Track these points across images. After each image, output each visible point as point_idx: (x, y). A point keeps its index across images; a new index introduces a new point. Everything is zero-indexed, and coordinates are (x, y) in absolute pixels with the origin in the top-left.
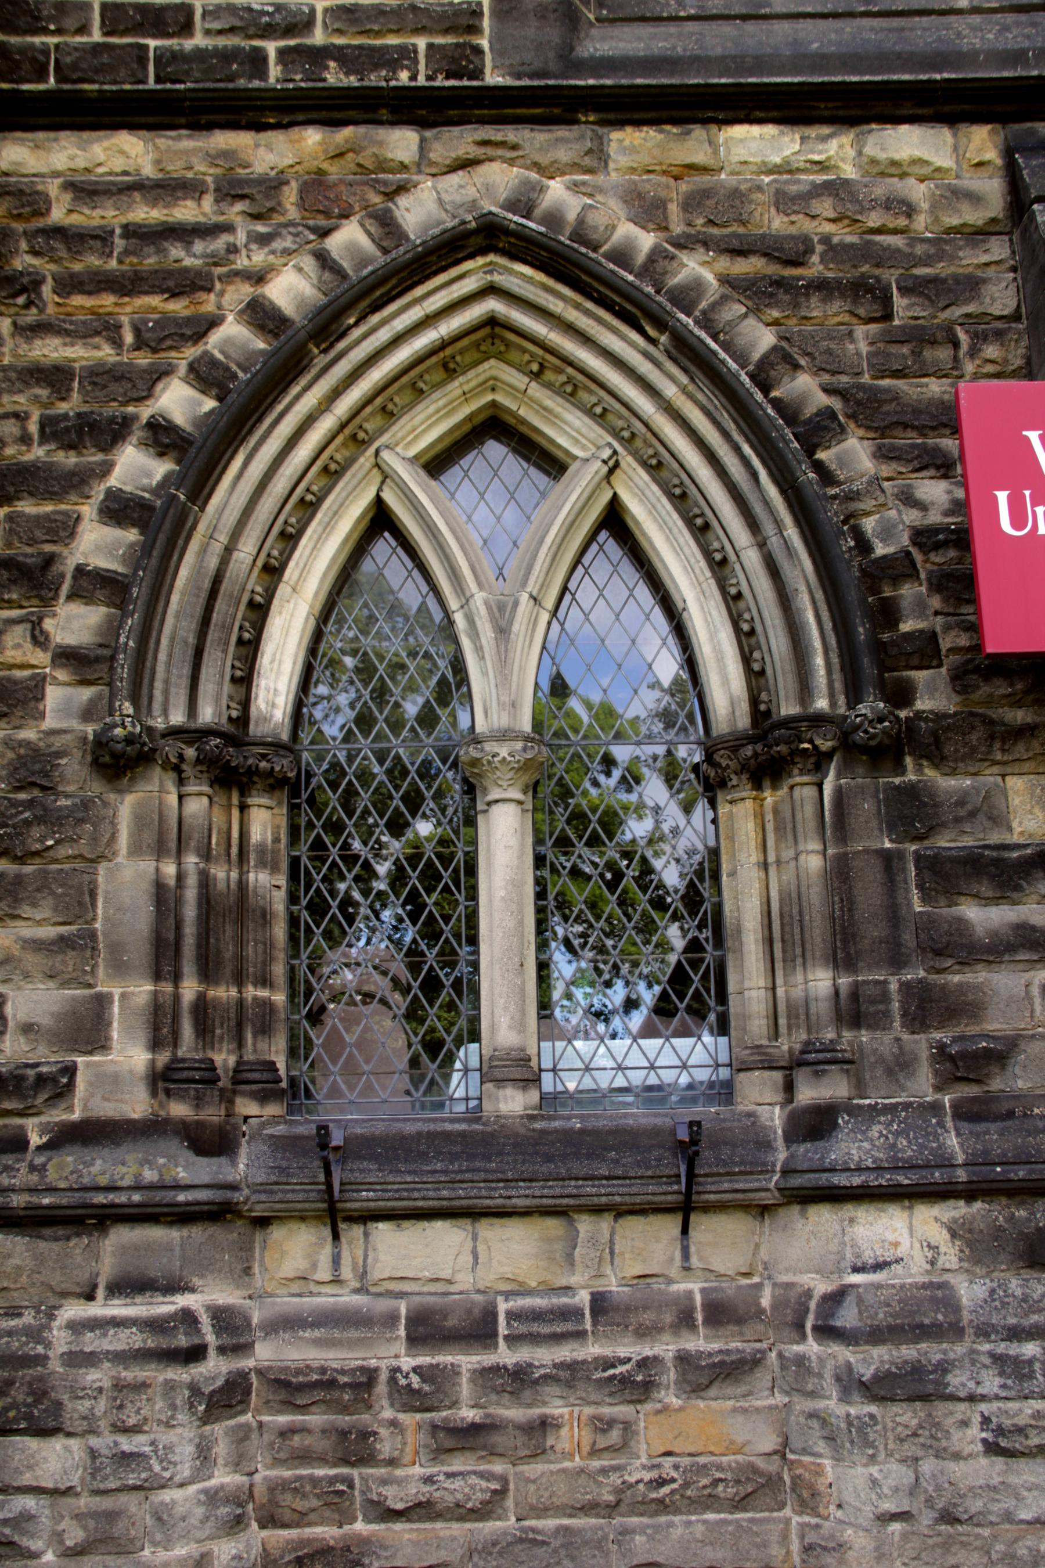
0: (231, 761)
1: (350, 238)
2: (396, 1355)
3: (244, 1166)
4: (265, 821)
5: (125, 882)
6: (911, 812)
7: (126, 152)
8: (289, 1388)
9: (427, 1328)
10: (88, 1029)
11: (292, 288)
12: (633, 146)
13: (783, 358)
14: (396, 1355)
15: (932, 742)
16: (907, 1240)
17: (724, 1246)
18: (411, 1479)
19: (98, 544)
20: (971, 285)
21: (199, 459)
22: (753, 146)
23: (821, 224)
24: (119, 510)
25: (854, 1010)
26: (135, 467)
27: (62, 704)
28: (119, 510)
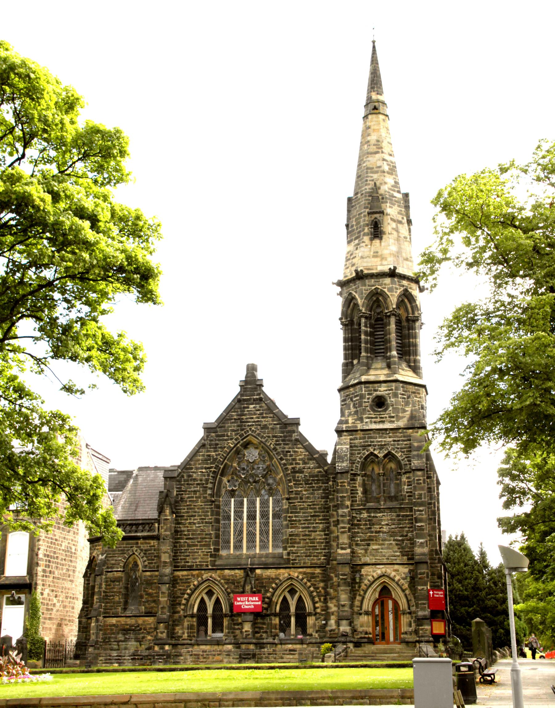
0: (192, 616)
1: (200, 579)
2: (201, 653)
3: (193, 642)
4: (195, 619)
5: (186, 624)
6: (233, 620)
7: (185, 573)
8: (195, 655)
9: (203, 652)
10: (183, 633)
11: (196, 583)
12: (218, 572)
13: (228, 588)
14: (201, 653)
15: (234, 616)
16: (230, 647)
17: (220, 647)
18: (202, 660)
19: (184, 602)
21: (190, 595)
22: (227, 572)
23: (231, 578)
24: (185, 599)
25: (229, 633)
27: (182, 612)
28: (185, 599)
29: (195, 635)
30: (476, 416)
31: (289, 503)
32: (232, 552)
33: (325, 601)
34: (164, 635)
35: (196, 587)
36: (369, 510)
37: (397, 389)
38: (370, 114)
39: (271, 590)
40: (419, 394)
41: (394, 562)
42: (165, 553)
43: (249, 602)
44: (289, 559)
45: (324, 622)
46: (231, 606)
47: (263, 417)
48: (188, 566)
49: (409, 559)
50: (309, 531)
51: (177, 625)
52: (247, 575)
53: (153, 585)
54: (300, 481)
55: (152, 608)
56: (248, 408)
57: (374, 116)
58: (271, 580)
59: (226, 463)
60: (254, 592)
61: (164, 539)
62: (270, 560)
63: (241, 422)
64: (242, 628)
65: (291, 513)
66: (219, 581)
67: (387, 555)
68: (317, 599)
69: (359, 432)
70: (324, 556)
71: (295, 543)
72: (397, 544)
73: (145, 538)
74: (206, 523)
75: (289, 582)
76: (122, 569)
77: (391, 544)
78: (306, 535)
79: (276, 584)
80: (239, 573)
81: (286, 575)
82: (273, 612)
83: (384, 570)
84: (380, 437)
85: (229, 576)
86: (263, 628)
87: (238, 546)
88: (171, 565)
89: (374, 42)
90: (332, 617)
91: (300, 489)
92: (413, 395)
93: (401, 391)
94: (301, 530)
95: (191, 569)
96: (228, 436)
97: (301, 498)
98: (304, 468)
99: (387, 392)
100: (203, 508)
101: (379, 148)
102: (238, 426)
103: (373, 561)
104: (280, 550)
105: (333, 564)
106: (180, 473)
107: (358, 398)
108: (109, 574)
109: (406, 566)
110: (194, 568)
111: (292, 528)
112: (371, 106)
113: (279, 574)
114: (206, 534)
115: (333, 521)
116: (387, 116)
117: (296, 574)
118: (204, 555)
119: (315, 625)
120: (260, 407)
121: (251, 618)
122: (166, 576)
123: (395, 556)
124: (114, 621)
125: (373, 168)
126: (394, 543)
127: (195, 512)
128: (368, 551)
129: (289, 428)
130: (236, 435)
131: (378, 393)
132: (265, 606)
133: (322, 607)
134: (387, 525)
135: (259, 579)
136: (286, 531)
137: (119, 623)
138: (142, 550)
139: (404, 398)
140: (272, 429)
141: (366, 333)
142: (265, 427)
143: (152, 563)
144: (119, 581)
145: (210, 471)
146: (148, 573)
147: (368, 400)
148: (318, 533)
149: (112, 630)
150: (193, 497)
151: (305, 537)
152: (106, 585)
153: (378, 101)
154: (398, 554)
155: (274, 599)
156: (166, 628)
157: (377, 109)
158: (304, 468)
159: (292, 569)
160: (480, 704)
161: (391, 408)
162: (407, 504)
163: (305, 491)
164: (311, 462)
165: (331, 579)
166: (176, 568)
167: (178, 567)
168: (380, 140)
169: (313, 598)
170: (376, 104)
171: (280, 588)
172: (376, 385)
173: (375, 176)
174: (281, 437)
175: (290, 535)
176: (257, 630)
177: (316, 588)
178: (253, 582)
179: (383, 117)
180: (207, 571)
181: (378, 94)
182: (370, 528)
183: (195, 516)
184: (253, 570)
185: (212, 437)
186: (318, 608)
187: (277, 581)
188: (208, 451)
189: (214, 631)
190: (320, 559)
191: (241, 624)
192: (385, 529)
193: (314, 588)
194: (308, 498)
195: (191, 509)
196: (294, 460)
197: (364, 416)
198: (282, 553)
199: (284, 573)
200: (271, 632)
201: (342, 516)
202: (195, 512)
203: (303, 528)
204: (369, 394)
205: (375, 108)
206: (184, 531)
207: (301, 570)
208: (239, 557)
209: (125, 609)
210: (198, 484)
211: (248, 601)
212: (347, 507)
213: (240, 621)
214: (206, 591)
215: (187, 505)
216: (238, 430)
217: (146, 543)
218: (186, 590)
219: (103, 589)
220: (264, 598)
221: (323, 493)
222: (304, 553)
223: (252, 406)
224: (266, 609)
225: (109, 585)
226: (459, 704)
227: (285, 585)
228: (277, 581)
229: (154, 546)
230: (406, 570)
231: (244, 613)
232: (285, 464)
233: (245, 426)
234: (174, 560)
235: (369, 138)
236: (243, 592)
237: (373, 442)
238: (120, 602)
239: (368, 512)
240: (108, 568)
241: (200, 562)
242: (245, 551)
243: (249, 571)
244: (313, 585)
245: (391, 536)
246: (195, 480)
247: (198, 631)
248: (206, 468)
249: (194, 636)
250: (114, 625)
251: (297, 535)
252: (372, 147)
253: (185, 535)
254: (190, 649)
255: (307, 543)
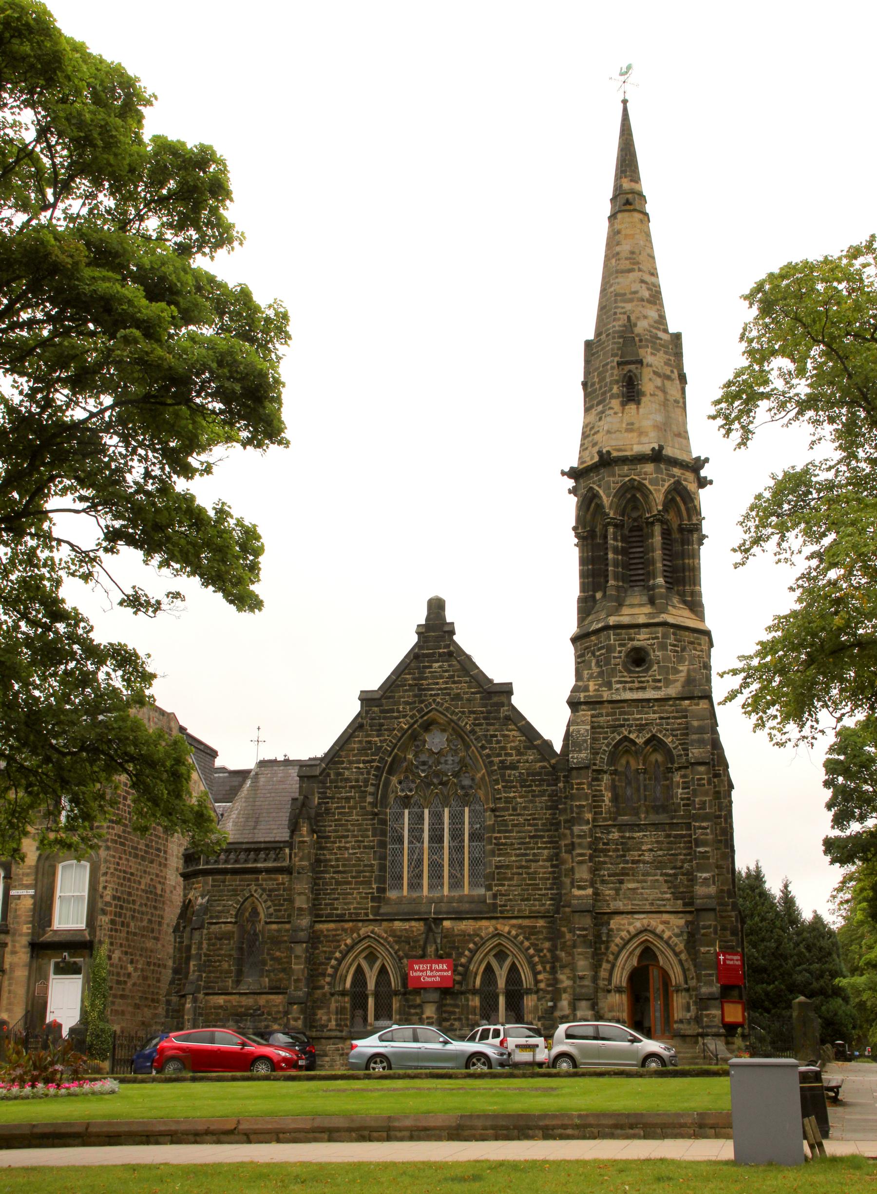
0: (343, 993)
1: (355, 935)
3: (344, 1034)
4: (347, 999)
5: (333, 1006)
6: (407, 1000)
7: (332, 926)
10: (330, 1020)
11: (349, 941)
12: (385, 924)
13: (399, 950)
15: (410, 993)
19: (330, 971)
20: (418, 941)
21: (340, 961)
22: (397, 924)
23: (404, 933)
24: (332, 967)
26: (333, 962)
27: (327, 988)
28: (332, 967)
29: (348, 1023)
30: (817, 657)
31: (496, 816)
32: (405, 893)
33: (553, 971)
34: (300, 1024)
35: (350, 948)
36: (621, 827)
37: (665, 636)
38: (620, 211)
39: (467, 953)
40: (700, 644)
41: (662, 909)
42: (300, 894)
43: (432, 973)
44: (495, 905)
45: (550, 1004)
46: (405, 978)
47: (454, 682)
48: (337, 916)
49: (685, 905)
50: (527, 861)
51: (320, 1008)
52: (429, 930)
53: (283, 945)
54: (512, 781)
55: (280, 980)
56: (431, 667)
57: (626, 214)
58: (467, 937)
59: (396, 754)
60: (441, 957)
61: (299, 873)
62: (466, 907)
63: (420, 689)
64: (422, 1013)
65: (499, 832)
66: (386, 939)
67: (651, 897)
68: (539, 968)
69: (606, 705)
70: (551, 899)
71: (505, 879)
72: (666, 881)
73: (268, 871)
74: (365, 847)
75: (496, 941)
76: (233, 920)
77: (657, 880)
78: (521, 867)
79: (475, 943)
80: (417, 927)
81: (491, 929)
82: (471, 987)
83: (645, 922)
84: (639, 713)
85: (401, 930)
86: (454, 1013)
87: (415, 885)
88: (310, 914)
89: (625, 102)
90: (564, 996)
91: (512, 795)
92: (691, 646)
93: (671, 640)
94: (514, 858)
95: (341, 919)
96: (399, 712)
97: (515, 809)
98: (519, 762)
99: (649, 642)
100: (360, 825)
101: (634, 264)
102: (415, 696)
103: (629, 908)
104: (482, 891)
105: (564, 913)
106: (324, 769)
107: (603, 651)
108: (213, 927)
109: (681, 915)
110: (347, 917)
111: (499, 855)
112: (621, 200)
113: (480, 928)
114: (365, 866)
115: (566, 845)
116: (647, 215)
117: (507, 929)
118: (361, 898)
119: (536, 1007)
120: (450, 666)
121: (435, 996)
122: (302, 930)
123: (663, 900)
124: (220, 1000)
125: (625, 294)
126: (661, 878)
127: (348, 831)
128: (621, 892)
129: (495, 699)
130: (411, 709)
131: (636, 643)
132: (458, 978)
133: (548, 979)
134: (651, 850)
135: (447, 935)
136: (491, 861)
137: (229, 1005)
138: (264, 890)
139: (677, 652)
140: (468, 700)
141: (616, 551)
142: (457, 697)
143: (280, 911)
144: (229, 939)
145: (372, 767)
146: (274, 926)
147: (619, 655)
148: (541, 863)
149: (218, 1014)
150: (344, 807)
151: (520, 871)
152: (209, 945)
153: (633, 192)
154: (668, 896)
155: (471, 967)
156: (303, 1011)
157: (630, 204)
158: (519, 762)
159: (501, 921)
160: (832, 1139)
161: (655, 667)
162: (682, 817)
163: (521, 797)
164: (530, 752)
165: (561, 935)
166: (317, 917)
167: (321, 916)
168: (637, 251)
169: (532, 966)
170: (630, 196)
171: (481, 950)
172: (632, 631)
173: (629, 307)
174: (482, 712)
175: (497, 867)
176: (444, 1015)
177: (539, 950)
178: (439, 941)
179: (641, 216)
180: (367, 924)
181: (631, 181)
182: (624, 856)
183: (347, 836)
184: (438, 921)
185: (374, 712)
186: (541, 981)
187: (477, 939)
188: (368, 736)
189: (377, 1018)
190: (544, 905)
191: (420, 1006)
192: (648, 857)
193: (535, 950)
194: (525, 808)
195: (341, 825)
196: (504, 748)
197: (614, 680)
198: (485, 895)
199: (487, 927)
200: (467, 1019)
201: (579, 836)
202: (348, 831)
203: (517, 855)
204: (621, 645)
205: (628, 202)
206: (330, 860)
207: (514, 921)
208: (417, 901)
209: (238, 982)
210: (352, 787)
211: (431, 970)
212: (588, 822)
213: (418, 1001)
214: (364, 954)
215: (336, 820)
216: (415, 702)
217: (271, 879)
218: (334, 953)
219: (205, 950)
220: (456, 966)
221: (549, 801)
222: (519, 895)
223: (436, 665)
224: (460, 983)
225: (214, 945)
226: (813, 1141)
227: (490, 945)
228: (477, 939)
229: (283, 884)
230: (682, 922)
231: (425, 989)
232: (488, 756)
233: (425, 695)
234: (314, 905)
235: (618, 249)
236: (423, 956)
237: (628, 720)
238: (229, 972)
239: (620, 831)
240: (211, 917)
241: (355, 908)
242: (425, 891)
243: (432, 923)
244: (533, 945)
245: (657, 868)
246: (347, 780)
247: (353, 1017)
248: (364, 762)
249: (346, 1026)
250: (221, 1007)
251: (507, 867)
252: (622, 261)
253: (332, 866)
254: (340, 1046)
255: (524, 879)
